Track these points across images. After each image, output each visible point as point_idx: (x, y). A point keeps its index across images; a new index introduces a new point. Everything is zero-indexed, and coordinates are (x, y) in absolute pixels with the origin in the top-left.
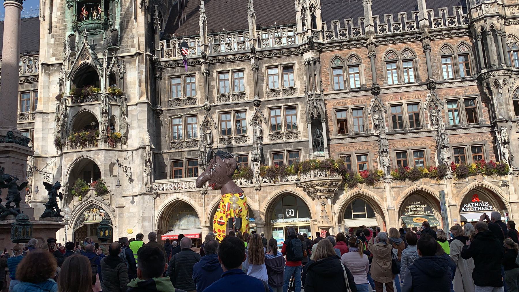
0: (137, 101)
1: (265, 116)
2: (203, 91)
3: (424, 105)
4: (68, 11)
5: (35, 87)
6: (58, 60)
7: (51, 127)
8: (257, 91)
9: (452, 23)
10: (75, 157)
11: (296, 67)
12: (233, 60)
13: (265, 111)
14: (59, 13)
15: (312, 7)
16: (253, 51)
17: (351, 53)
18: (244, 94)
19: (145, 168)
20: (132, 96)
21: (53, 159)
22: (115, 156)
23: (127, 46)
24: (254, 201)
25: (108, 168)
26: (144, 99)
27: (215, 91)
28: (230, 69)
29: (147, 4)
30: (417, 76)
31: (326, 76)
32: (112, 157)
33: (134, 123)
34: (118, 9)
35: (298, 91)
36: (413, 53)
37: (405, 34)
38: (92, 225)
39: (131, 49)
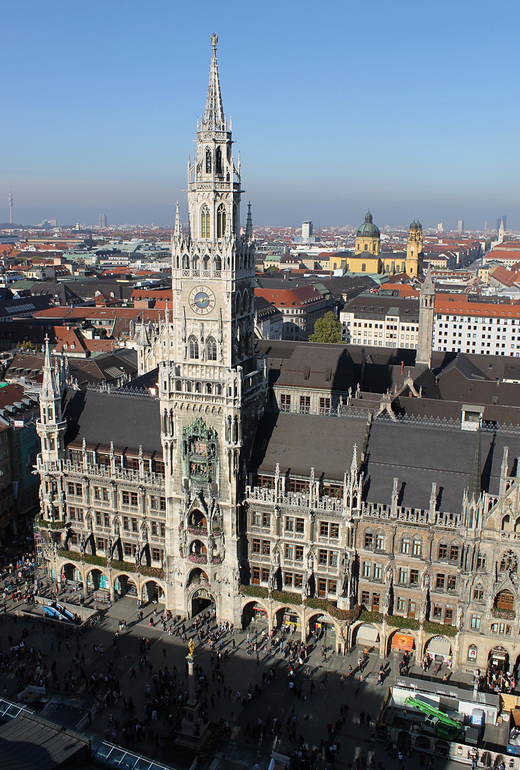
1: (316, 554)
2: (275, 527)
4: (183, 461)
14: (177, 461)
15: (355, 492)
17: (379, 527)
19: (235, 581)
22: (217, 568)
23: (224, 497)
24: (301, 614)
25: (213, 577)
27: (283, 529)
28: (295, 516)
29: (238, 472)
31: (360, 538)
32: (215, 570)
34: (218, 469)
35: (339, 543)
37: (417, 525)
38: (203, 599)
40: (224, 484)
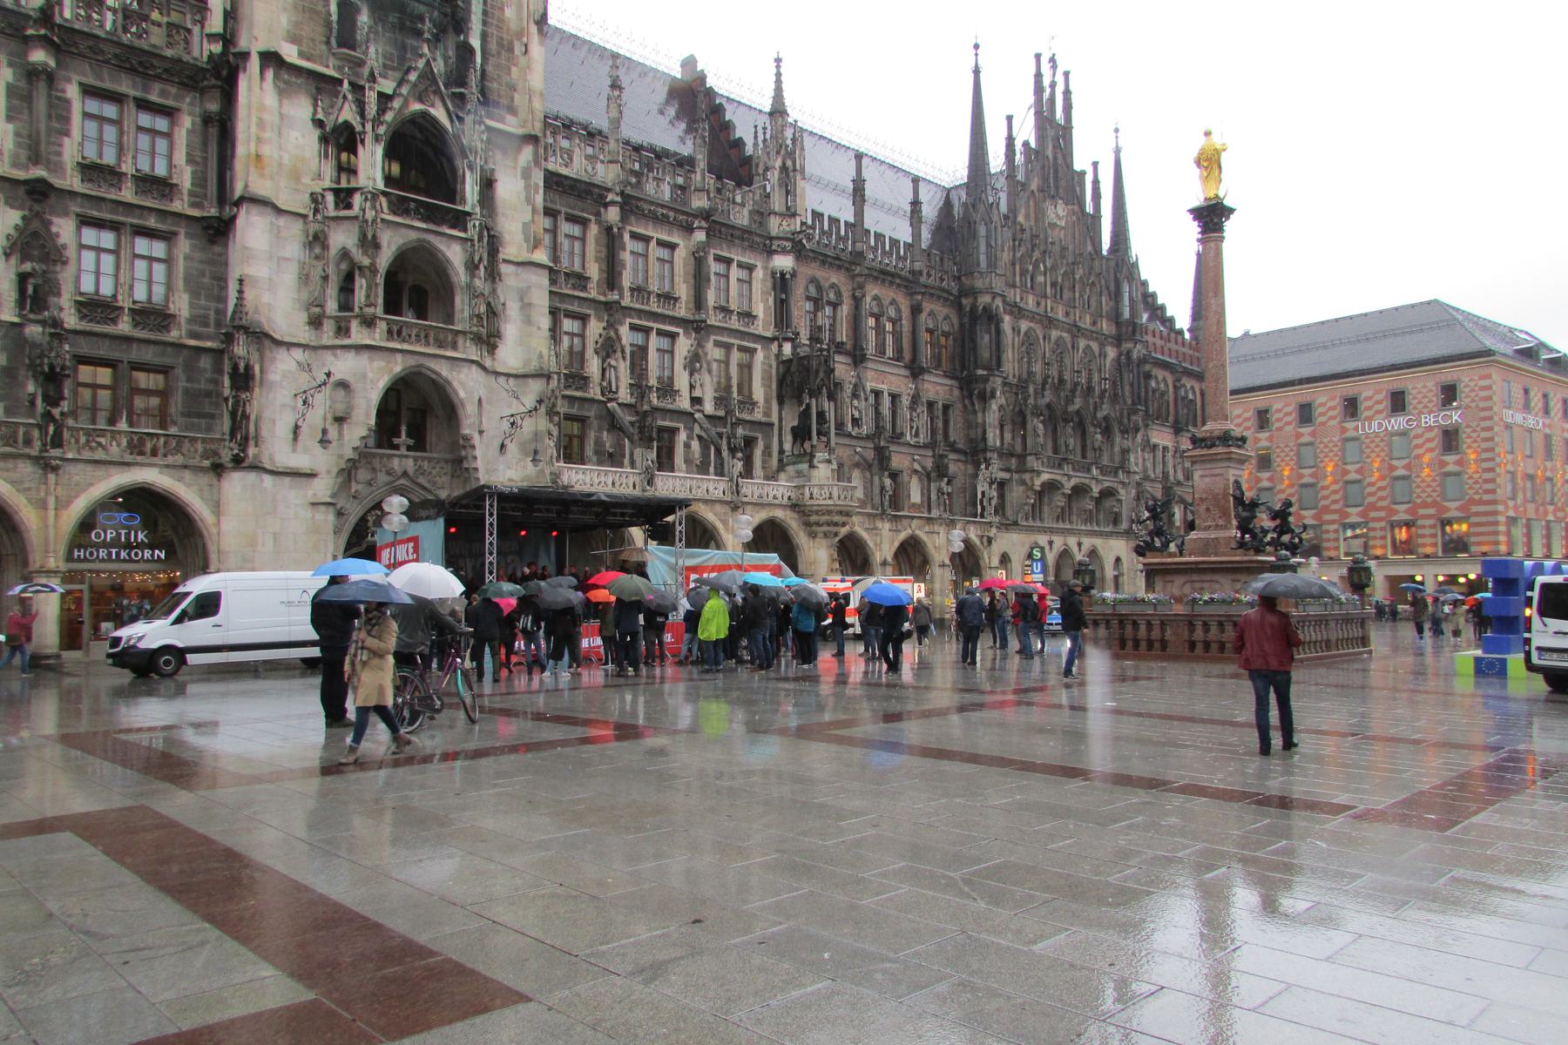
0: (524, 256)
3: (905, 401)
5: (146, 89)
6: (308, 59)
7: (287, 255)
8: (699, 302)
9: (942, 280)
10: (398, 366)
11: (759, 274)
12: (661, 221)
13: (710, 345)
16: (706, 215)
18: (676, 300)
20: (507, 237)
21: (298, 354)
26: (542, 256)
30: (899, 350)
33: (513, 309)
35: (760, 322)
36: (898, 310)
39: (509, 118)
40: (499, 53)
